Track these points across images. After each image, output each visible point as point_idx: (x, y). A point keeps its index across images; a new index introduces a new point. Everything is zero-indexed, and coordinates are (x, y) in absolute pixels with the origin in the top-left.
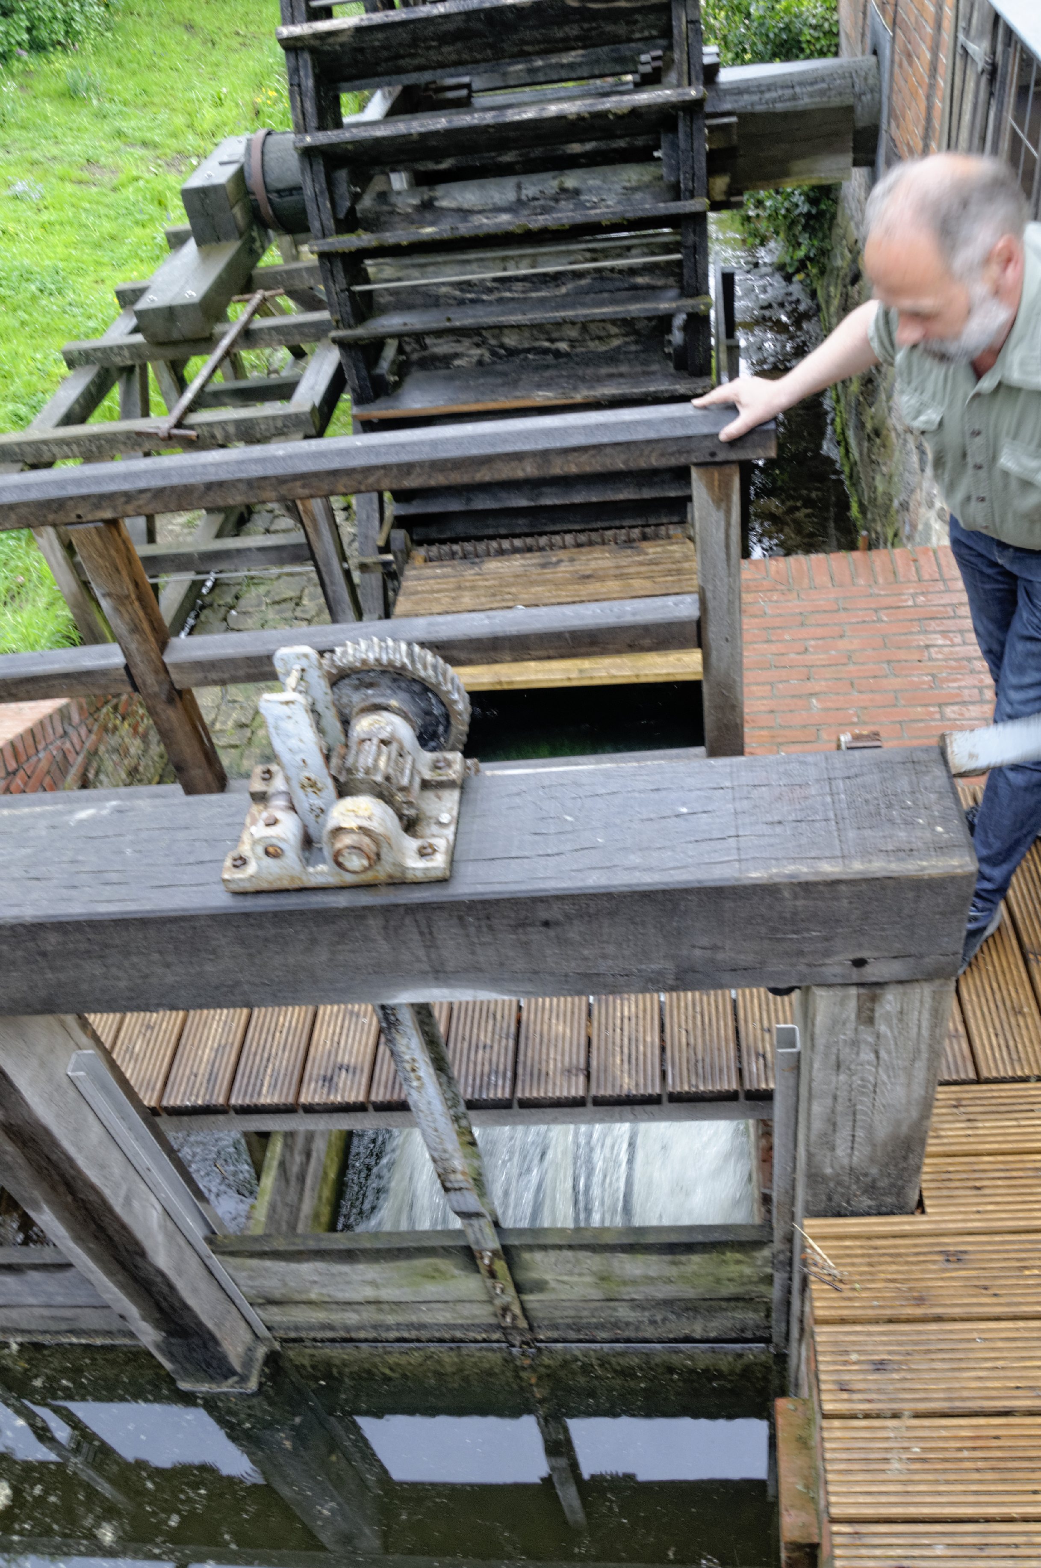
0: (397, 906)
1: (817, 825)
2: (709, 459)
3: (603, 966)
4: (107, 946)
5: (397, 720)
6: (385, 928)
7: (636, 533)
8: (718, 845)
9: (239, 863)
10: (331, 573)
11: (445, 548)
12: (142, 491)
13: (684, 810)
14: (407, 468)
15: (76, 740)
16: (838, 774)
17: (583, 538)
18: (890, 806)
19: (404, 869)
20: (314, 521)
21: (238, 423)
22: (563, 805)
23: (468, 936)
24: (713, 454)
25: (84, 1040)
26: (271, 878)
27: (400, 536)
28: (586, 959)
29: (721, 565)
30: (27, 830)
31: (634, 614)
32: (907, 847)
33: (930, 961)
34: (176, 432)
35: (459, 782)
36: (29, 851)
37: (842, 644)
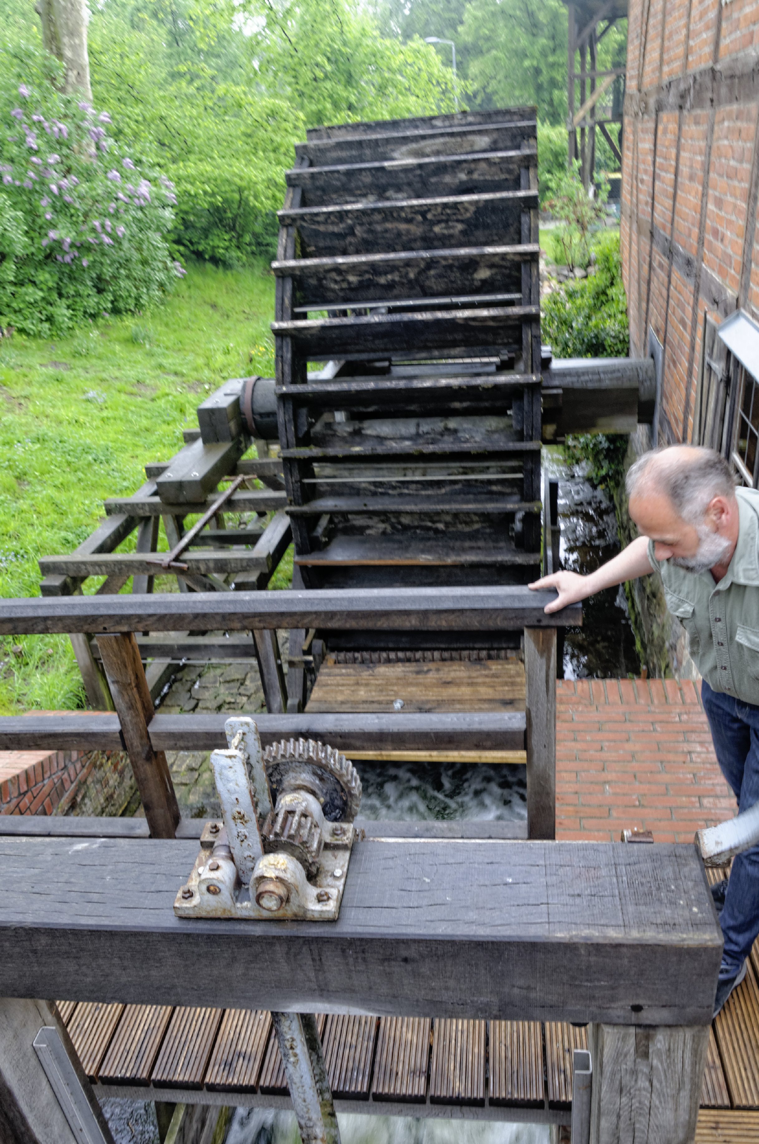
0: (298, 937)
1: (606, 899)
2: (536, 623)
3: (445, 996)
4: (82, 950)
5: (310, 798)
6: (287, 953)
7: (484, 654)
10: (268, 666)
11: (350, 655)
12: (150, 616)
13: (510, 880)
14: (331, 615)
15: (72, 772)
16: (621, 861)
17: (446, 655)
18: (659, 889)
19: (306, 910)
21: (216, 561)
22: (423, 869)
23: (347, 964)
24: (539, 621)
25: (50, 1017)
26: (209, 909)
27: (319, 644)
28: (433, 989)
29: (543, 694)
31: (480, 723)
32: (671, 922)
33: (691, 1011)
34: (174, 564)
35: (350, 846)
36: (36, 871)
37: (629, 747)
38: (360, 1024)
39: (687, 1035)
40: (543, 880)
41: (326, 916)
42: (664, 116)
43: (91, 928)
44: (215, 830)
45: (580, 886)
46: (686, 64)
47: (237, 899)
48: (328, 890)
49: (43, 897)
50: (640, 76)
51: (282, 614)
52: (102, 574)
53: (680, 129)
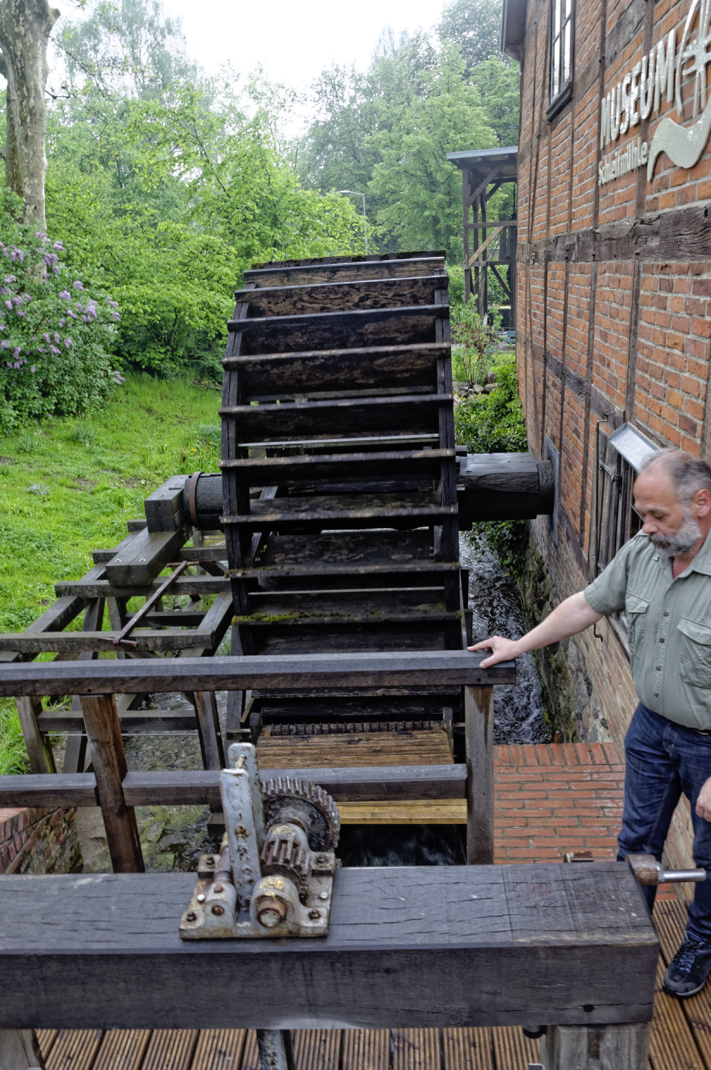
0: (292, 953)
2: (477, 683)
5: (298, 829)
6: (282, 969)
8: (499, 920)
9: (191, 918)
10: (209, 738)
11: (285, 727)
12: (132, 678)
13: (475, 897)
15: (18, 842)
16: (568, 877)
17: (375, 725)
19: (299, 927)
20: (203, 703)
21: (164, 638)
23: (335, 978)
24: (479, 680)
26: (212, 929)
28: (411, 999)
29: (482, 746)
30: (45, 890)
31: (427, 774)
32: (615, 925)
36: (45, 904)
37: (548, 804)
38: (324, 1061)
39: (631, 1032)
40: (503, 896)
41: (318, 932)
42: (553, 265)
43: (101, 953)
44: (211, 862)
45: (536, 899)
47: (237, 919)
48: (319, 909)
49: (54, 926)
50: (530, 231)
51: (253, 676)
52: (54, 651)
53: (567, 275)
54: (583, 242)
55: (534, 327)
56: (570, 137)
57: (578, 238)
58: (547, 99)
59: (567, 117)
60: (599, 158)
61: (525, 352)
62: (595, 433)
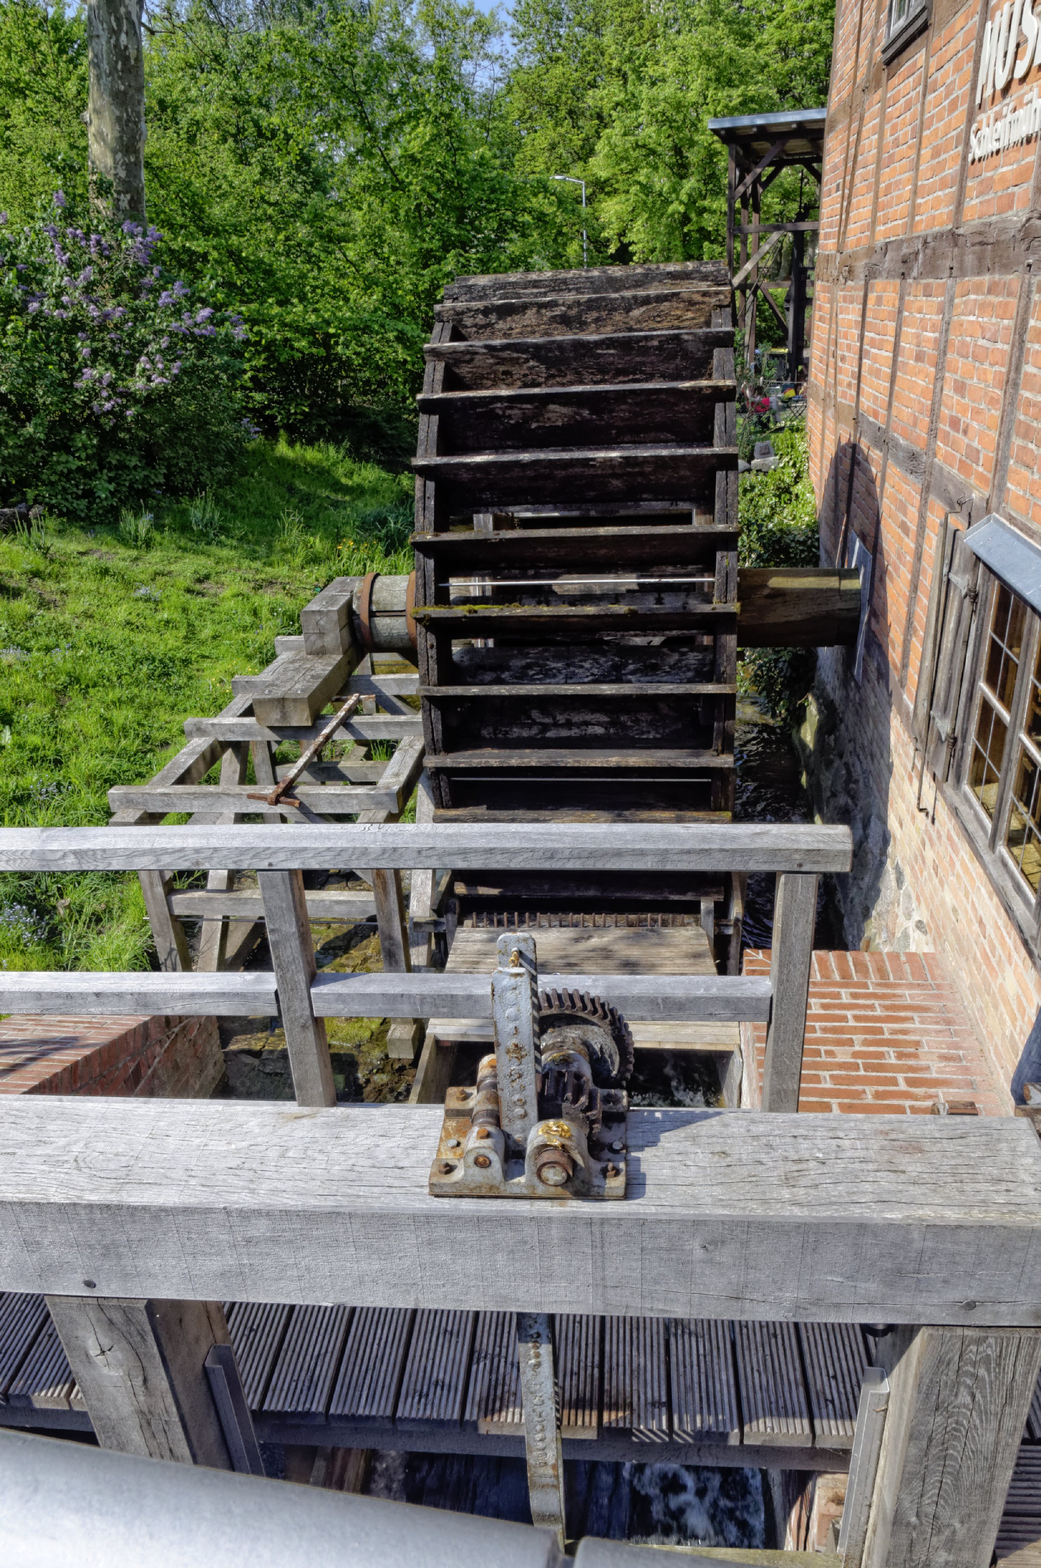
2: (796, 869)
12: (329, 849)
42: (878, 284)
46: (912, 225)
50: (842, 234)
53: (902, 298)
54: (934, 249)
55: (839, 376)
56: (920, 89)
57: (925, 243)
58: (884, 29)
59: (918, 57)
60: (970, 121)
61: (824, 412)
62: (939, 530)
